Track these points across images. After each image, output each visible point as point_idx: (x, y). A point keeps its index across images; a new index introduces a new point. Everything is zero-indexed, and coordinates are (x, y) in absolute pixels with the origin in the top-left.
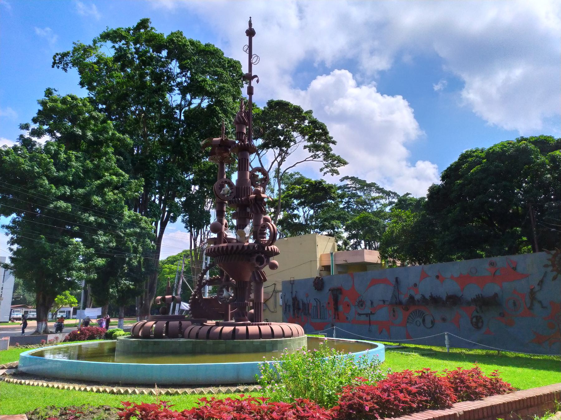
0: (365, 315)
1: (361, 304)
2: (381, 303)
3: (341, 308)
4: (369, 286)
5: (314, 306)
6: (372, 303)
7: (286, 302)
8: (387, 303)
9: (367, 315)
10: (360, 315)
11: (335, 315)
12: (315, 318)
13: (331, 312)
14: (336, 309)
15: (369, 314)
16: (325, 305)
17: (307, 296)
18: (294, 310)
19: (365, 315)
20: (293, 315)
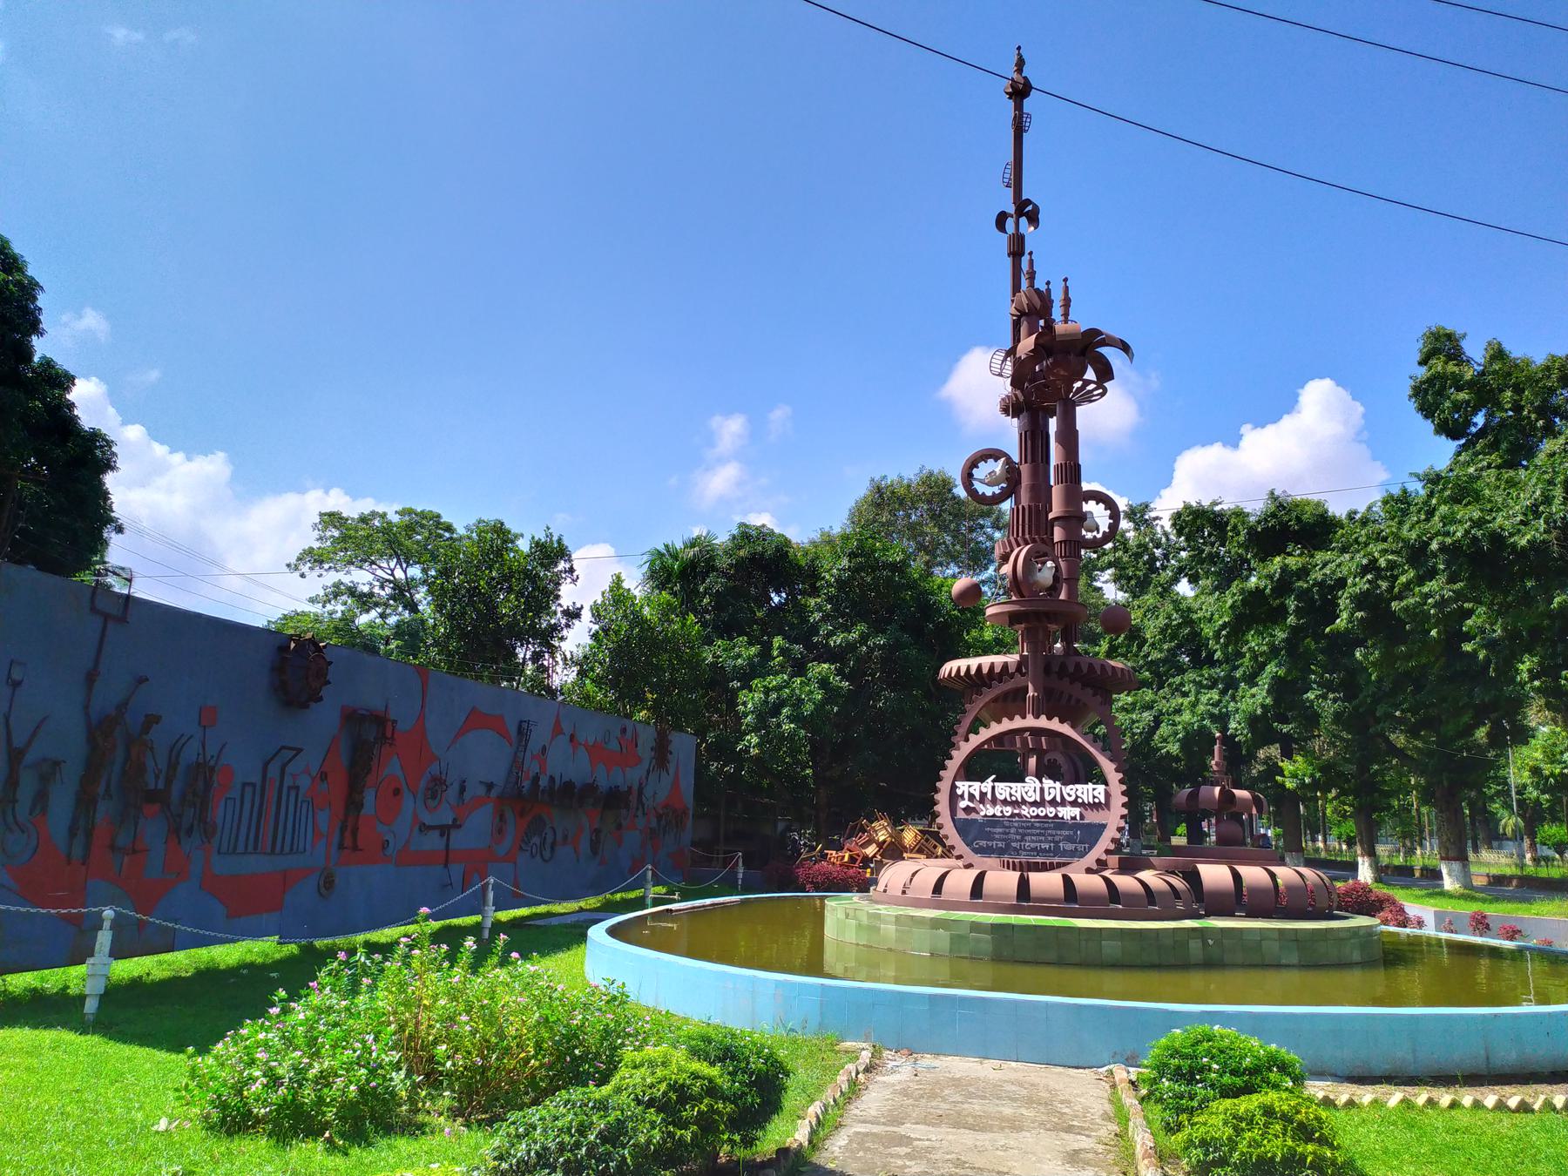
0: (437, 833)
1: (437, 786)
2: (481, 791)
3: (369, 797)
4: (462, 732)
5: (244, 785)
6: (463, 789)
7: (19, 741)
8: (494, 794)
9: (444, 830)
10: (424, 828)
11: (343, 830)
12: (241, 848)
13: (323, 818)
14: (353, 803)
15: (449, 827)
16: (305, 782)
17: (207, 717)
18: (85, 800)
19: (437, 833)
20: (72, 832)
